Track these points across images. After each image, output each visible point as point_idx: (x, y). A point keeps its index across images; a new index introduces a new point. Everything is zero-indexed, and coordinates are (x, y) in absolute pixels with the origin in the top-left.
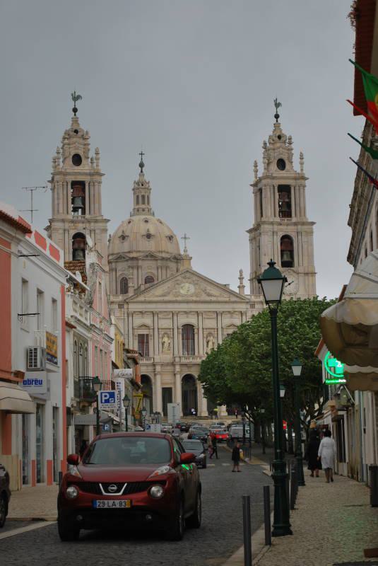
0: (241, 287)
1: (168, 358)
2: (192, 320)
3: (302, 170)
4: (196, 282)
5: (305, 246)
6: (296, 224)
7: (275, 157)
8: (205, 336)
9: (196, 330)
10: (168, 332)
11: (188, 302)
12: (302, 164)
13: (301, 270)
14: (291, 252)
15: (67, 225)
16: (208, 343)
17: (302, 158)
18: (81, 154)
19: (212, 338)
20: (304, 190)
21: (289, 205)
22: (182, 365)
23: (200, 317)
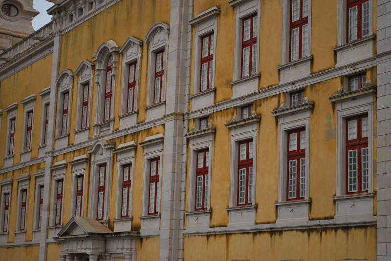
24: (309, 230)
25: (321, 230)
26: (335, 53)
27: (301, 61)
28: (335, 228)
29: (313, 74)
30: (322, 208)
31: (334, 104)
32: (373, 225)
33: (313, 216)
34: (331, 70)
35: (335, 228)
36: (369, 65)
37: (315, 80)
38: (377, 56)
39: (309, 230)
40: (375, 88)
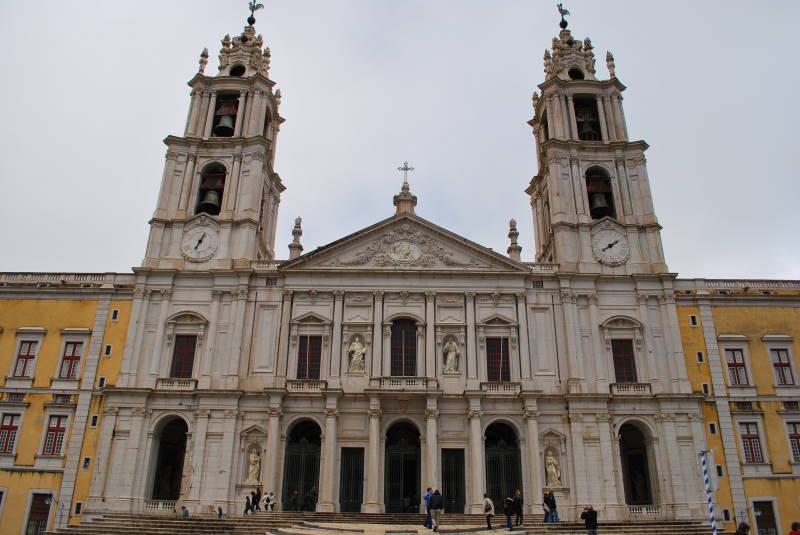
0: (515, 249)
1: (356, 384)
2: (414, 310)
3: (613, 74)
4: (422, 239)
5: (634, 183)
6: (612, 147)
7: (567, 63)
8: (439, 341)
9: (420, 329)
10: (357, 332)
11: (404, 275)
12: (611, 67)
13: (628, 221)
14: (609, 197)
15: (193, 150)
16: (445, 356)
17: (610, 58)
18: (246, 62)
19: (454, 343)
20: (620, 103)
21: (596, 126)
22: (384, 398)
23: (430, 305)
24: (12, 471)
25: (21, 471)
26: (52, 381)
27: (28, 379)
28: (33, 471)
29: (33, 388)
30: (25, 460)
31: (45, 408)
32: (62, 472)
33: (17, 463)
34: (48, 389)
35: (33, 471)
36: (74, 393)
37: (34, 392)
38: (79, 389)
39: (12, 471)
40: (76, 405)
